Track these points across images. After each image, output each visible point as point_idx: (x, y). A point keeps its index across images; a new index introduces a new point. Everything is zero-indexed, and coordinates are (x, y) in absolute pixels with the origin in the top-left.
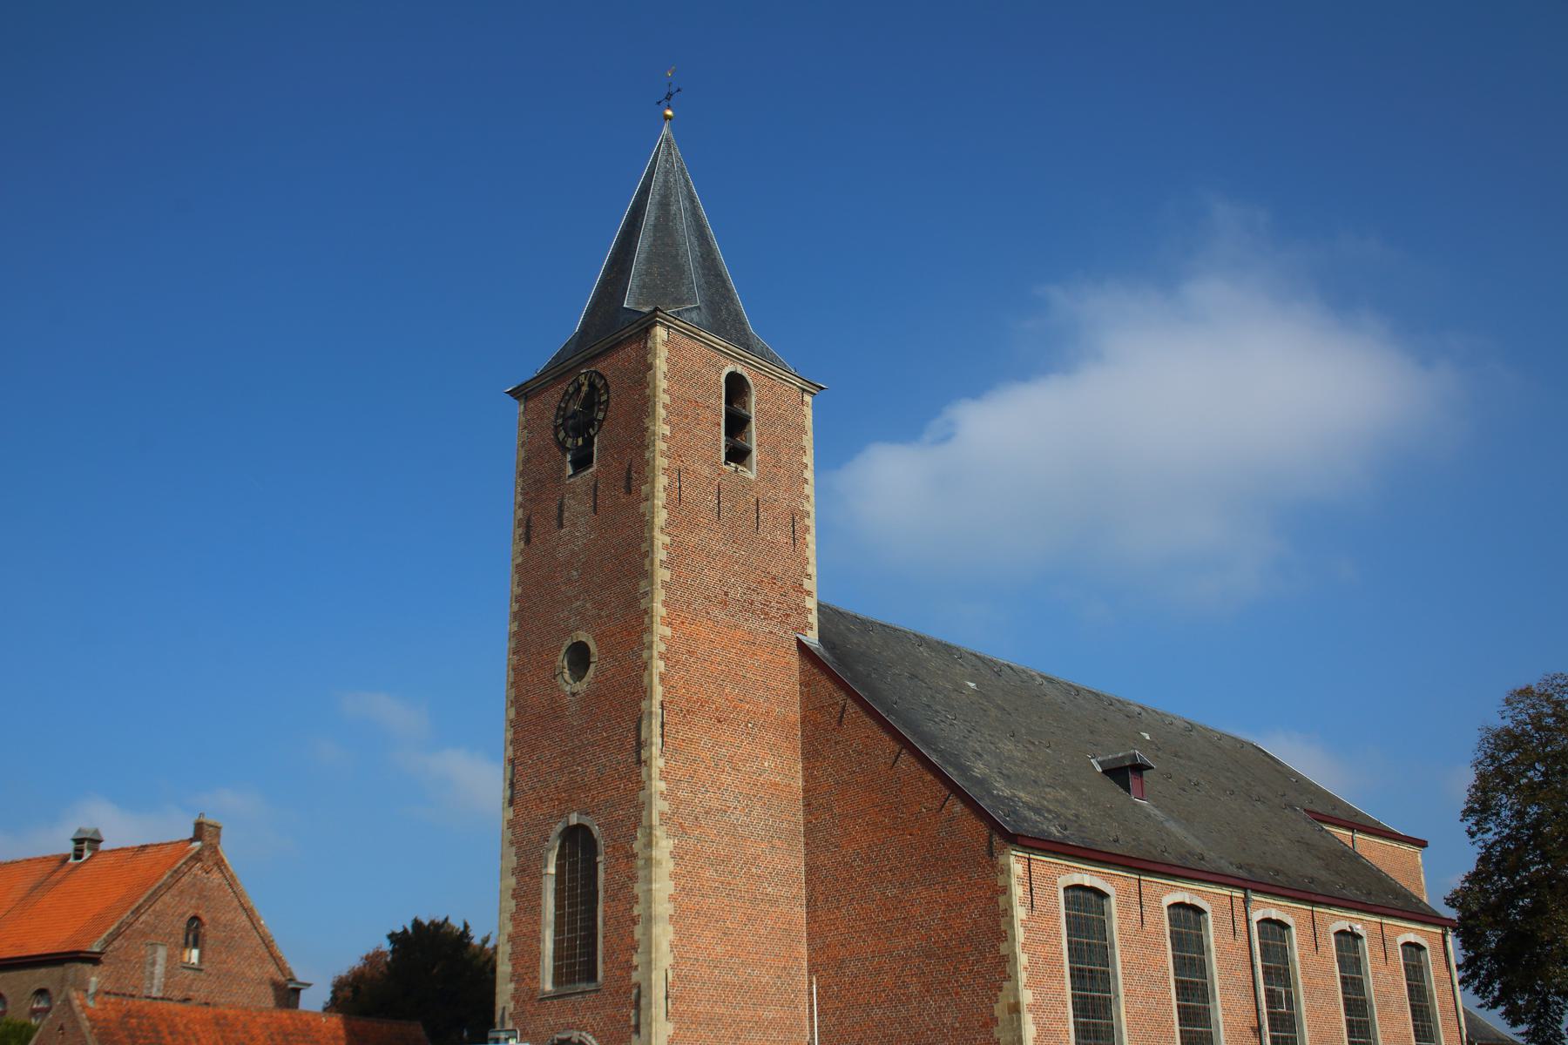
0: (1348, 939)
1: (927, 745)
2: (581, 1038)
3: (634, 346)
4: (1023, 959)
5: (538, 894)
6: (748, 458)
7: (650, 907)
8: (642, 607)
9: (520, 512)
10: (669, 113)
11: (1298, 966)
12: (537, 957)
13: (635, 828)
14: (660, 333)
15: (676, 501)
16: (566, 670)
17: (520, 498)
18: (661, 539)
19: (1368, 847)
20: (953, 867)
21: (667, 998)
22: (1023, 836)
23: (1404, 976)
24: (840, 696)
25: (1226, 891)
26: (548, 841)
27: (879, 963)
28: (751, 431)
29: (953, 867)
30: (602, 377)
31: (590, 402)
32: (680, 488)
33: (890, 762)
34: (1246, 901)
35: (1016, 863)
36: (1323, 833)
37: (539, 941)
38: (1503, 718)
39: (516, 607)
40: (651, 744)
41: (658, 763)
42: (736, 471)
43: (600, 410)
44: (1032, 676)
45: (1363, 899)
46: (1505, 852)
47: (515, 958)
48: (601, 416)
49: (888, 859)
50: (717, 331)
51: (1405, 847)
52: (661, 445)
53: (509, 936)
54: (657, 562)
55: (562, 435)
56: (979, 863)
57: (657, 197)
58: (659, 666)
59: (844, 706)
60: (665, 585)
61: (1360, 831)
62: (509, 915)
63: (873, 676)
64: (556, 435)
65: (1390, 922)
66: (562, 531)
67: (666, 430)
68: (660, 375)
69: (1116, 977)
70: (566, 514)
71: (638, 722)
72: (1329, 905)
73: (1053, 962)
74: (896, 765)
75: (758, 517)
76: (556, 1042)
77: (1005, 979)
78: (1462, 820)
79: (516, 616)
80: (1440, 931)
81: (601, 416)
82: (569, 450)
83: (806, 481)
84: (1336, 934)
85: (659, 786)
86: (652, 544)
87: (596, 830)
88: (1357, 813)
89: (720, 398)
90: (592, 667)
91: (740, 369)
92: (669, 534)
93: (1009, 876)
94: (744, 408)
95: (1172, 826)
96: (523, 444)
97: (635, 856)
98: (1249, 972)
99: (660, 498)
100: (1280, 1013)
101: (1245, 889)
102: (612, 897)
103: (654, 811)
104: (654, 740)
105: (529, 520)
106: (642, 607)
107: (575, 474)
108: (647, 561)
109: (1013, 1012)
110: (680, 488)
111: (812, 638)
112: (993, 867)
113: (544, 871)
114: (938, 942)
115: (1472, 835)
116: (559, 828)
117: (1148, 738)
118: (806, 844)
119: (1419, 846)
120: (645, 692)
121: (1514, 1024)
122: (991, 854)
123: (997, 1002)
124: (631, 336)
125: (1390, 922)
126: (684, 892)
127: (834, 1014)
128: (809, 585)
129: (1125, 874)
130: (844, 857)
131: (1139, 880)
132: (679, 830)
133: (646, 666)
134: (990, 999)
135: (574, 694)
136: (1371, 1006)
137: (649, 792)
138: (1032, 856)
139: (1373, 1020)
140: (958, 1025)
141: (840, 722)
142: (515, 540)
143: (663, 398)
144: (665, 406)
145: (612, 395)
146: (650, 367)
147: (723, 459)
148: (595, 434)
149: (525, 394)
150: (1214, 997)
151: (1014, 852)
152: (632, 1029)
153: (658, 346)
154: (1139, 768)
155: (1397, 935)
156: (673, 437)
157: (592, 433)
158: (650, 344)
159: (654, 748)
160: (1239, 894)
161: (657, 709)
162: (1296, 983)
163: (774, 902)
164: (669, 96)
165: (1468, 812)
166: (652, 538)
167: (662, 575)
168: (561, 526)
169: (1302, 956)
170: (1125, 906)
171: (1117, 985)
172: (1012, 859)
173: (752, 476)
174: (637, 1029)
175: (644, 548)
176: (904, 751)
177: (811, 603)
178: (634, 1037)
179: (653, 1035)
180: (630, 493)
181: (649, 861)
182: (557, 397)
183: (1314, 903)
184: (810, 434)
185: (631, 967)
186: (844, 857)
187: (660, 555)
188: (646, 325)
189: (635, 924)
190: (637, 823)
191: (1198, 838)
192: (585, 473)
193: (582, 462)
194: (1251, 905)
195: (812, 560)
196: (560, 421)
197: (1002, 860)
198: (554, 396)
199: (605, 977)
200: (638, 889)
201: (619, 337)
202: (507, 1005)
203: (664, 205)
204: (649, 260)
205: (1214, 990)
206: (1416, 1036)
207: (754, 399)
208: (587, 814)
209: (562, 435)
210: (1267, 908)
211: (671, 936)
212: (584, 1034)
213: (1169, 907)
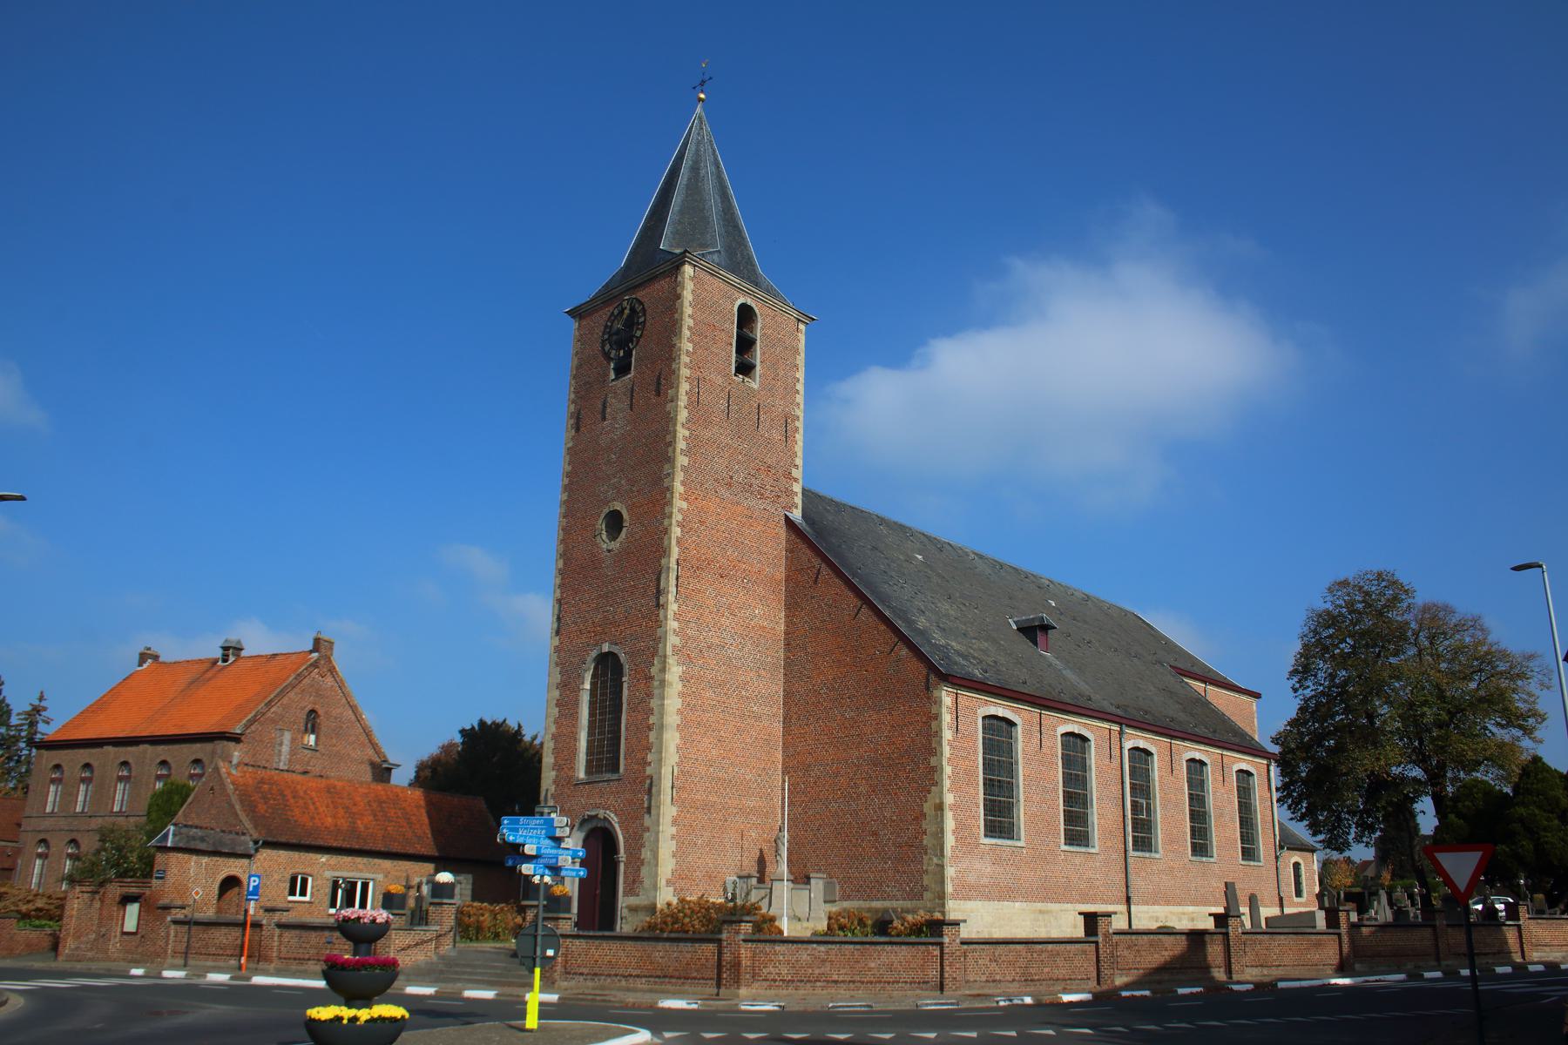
0: (1196, 765)
1: (883, 602)
3: (667, 280)
4: (948, 770)
5: (576, 703)
6: (753, 372)
7: (662, 718)
8: (665, 485)
9: (572, 407)
10: (702, 96)
11: (1157, 784)
12: (574, 752)
13: (653, 656)
14: (688, 270)
15: (695, 402)
16: (604, 532)
17: (573, 396)
18: (682, 432)
19: (1216, 696)
20: (898, 698)
21: (672, 788)
22: (953, 676)
23: (1236, 795)
24: (816, 562)
25: (1106, 725)
27: (837, 768)
28: (755, 351)
29: (898, 698)
30: (641, 303)
31: (631, 323)
32: (698, 393)
33: (853, 614)
34: (1121, 733)
35: (946, 696)
36: (1183, 684)
37: (575, 740)
38: (1325, 602)
39: (566, 481)
40: (668, 592)
41: (673, 607)
42: (743, 382)
43: (638, 329)
44: (967, 552)
45: (1210, 736)
46: (1318, 704)
47: (556, 751)
48: (638, 333)
49: (848, 689)
50: (733, 272)
51: (1244, 698)
52: (685, 359)
53: (553, 735)
54: (678, 451)
55: (607, 347)
56: (918, 695)
57: (690, 162)
58: (676, 532)
59: (819, 570)
60: (684, 468)
61: (1211, 684)
63: (843, 546)
64: (603, 347)
65: (1229, 754)
67: (690, 347)
68: (686, 303)
69: (1018, 786)
70: (608, 410)
71: (658, 573)
72: (1184, 739)
73: (970, 773)
75: (758, 419)
76: (586, 817)
77: (933, 785)
78: (1288, 679)
79: (567, 488)
80: (1266, 762)
81: (638, 333)
82: (612, 359)
83: (797, 392)
84: (1187, 761)
85: (673, 624)
86: (675, 437)
87: (622, 657)
88: (1210, 670)
89: (733, 323)
90: (624, 530)
91: (749, 302)
92: (689, 429)
93: (940, 706)
94: (751, 332)
95: (1068, 674)
96: (577, 353)
97: (652, 678)
98: (1120, 787)
99: (683, 400)
100: (1141, 819)
101: (1121, 724)
102: (632, 709)
103: (668, 644)
104: (670, 589)
105: (579, 414)
106: (665, 485)
108: (670, 449)
110: (698, 393)
111: (797, 515)
112: (929, 698)
115: (1295, 690)
116: (594, 654)
117: (1054, 605)
118: (785, 675)
119: (1254, 697)
120: (665, 552)
121: (1314, 834)
122: (927, 688)
123: (926, 801)
124: (665, 271)
125: (1229, 754)
126: (688, 707)
127: (800, 806)
128: (796, 473)
129: (1030, 709)
130: (814, 685)
131: (1041, 714)
132: (687, 659)
133: (666, 531)
134: (921, 799)
135: (609, 551)
136: (1210, 816)
138: (959, 691)
139: (1210, 827)
140: (895, 818)
141: (816, 582)
142: (567, 428)
143: (688, 322)
144: (690, 328)
145: (648, 317)
146: (679, 297)
147: (733, 372)
149: (580, 314)
150: (1092, 805)
151: (945, 688)
152: (645, 810)
153: (686, 280)
154: (1045, 628)
155: (1233, 763)
156: (695, 352)
157: (631, 346)
158: (679, 278)
159: (670, 595)
160: (1116, 728)
161: (673, 565)
162: (1155, 797)
163: (758, 718)
164: (702, 83)
165: (1293, 673)
166: (675, 431)
167: (682, 460)
168: (604, 419)
169: (1161, 777)
170: (1028, 733)
171: (1018, 793)
172: (944, 693)
173: (755, 386)
174: (649, 810)
175: (668, 438)
176: (864, 606)
177: (797, 488)
178: (646, 816)
179: (661, 816)
180: (659, 396)
181: (663, 683)
183: (1172, 737)
184: (803, 355)
185: (645, 763)
186: (814, 685)
187: (681, 445)
189: (650, 730)
190: (654, 653)
191: (1087, 683)
193: (622, 369)
194: (1125, 736)
195: (800, 454)
196: (606, 337)
197: (936, 693)
198: (602, 317)
199: (626, 770)
200: (654, 703)
203: (695, 169)
204: (682, 212)
205: (1092, 800)
206: (1241, 840)
207: (759, 325)
208: (616, 644)
210: (1136, 739)
211: (678, 741)
212: (608, 812)
213: (1062, 735)
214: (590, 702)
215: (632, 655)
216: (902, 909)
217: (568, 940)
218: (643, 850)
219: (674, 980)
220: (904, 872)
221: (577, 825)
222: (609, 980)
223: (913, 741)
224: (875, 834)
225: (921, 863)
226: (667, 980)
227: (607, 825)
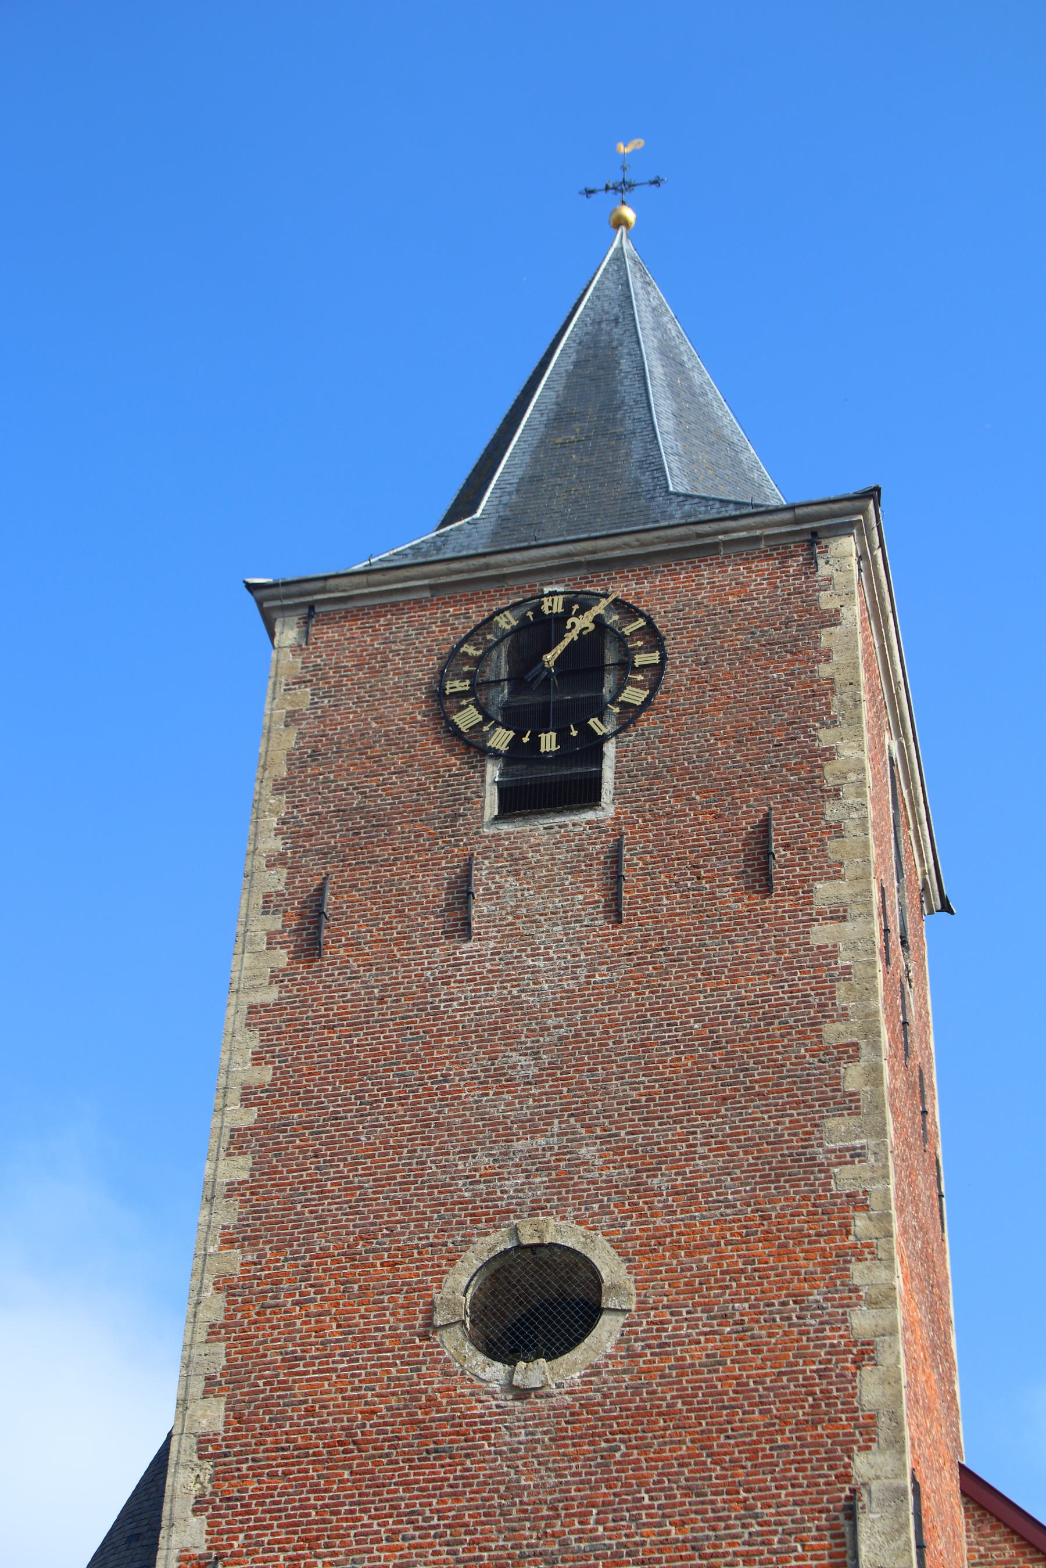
10: (629, 214)
48: (634, 695)
55: (467, 718)
66: (466, 947)
82: (496, 754)
124: (757, 539)
145: (675, 658)
148: (605, 738)
149: (311, 607)
168: (465, 930)
180: (767, 889)
182: (463, 627)
188: (816, 525)
192: (567, 819)
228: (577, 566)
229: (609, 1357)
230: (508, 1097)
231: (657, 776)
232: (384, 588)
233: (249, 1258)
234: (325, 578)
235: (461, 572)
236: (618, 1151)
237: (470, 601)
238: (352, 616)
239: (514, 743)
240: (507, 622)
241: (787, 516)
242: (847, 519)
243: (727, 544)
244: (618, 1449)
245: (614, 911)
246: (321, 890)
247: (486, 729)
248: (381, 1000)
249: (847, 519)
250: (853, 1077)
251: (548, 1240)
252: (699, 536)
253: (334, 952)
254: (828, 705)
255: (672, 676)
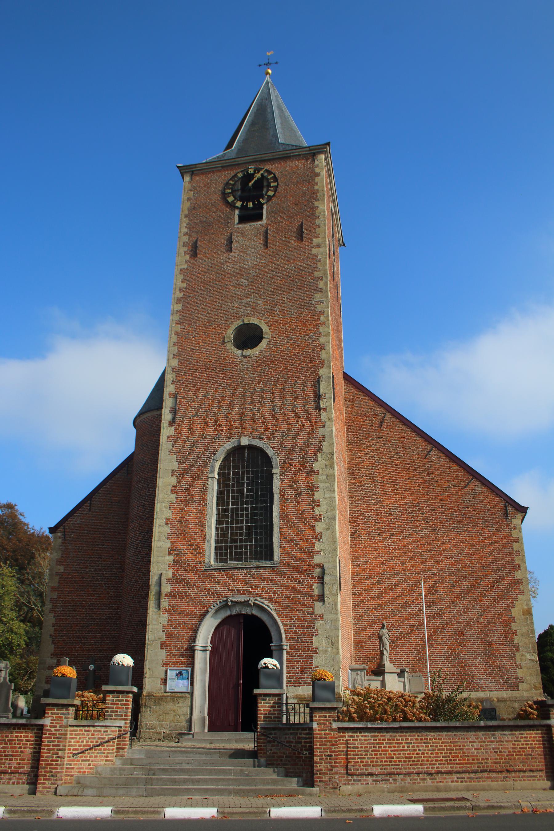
2: (257, 602)
5: (204, 490)
10: (270, 71)
13: (315, 453)
20: (477, 523)
24: (380, 411)
26: (215, 454)
29: (477, 523)
33: (423, 455)
37: (204, 526)
48: (271, 193)
49: (422, 513)
55: (231, 199)
62: (168, 505)
66: (231, 254)
74: (427, 457)
77: (519, 594)
82: (238, 208)
87: (270, 452)
97: (316, 472)
107: (238, 224)
109: (527, 615)
113: (210, 475)
114: (465, 567)
116: (228, 446)
123: (514, 607)
124: (300, 155)
130: (384, 508)
137: (329, 430)
140: (482, 620)
141: (380, 426)
148: (264, 204)
149: (193, 172)
168: (230, 250)
174: (321, 598)
176: (434, 449)
180: (302, 240)
182: (229, 177)
185: (313, 551)
186: (384, 508)
188: (315, 151)
189: (317, 520)
192: (255, 224)
201: (291, 153)
202: (164, 572)
208: (260, 439)
209: (231, 199)
212: (259, 599)
214: (219, 492)
215: (283, 450)
216: (498, 698)
217: (346, 734)
218: (315, 638)
219: (494, 775)
220: (497, 667)
221: (212, 612)
222: (408, 779)
223: (495, 557)
224: (461, 633)
225: (514, 658)
226: (485, 775)
227: (255, 612)
228: (257, 161)
229: (265, 348)
230: (241, 290)
231: (276, 213)
232: (210, 167)
233: (182, 327)
234: (196, 165)
235: (229, 163)
236: (267, 302)
237: (231, 170)
238: (203, 174)
239: (242, 205)
240: (240, 175)
241: (308, 149)
242: (322, 150)
243: (293, 156)
244: (267, 369)
245: (266, 245)
246: (196, 241)
247: (235, 201)
248: (211, 267)
249: (322, 150)
250: (321, 285)
251: (251, 322)
252: (287, 154)
253: (200, 256)
254: (317, 196)
255: (280, 189)
